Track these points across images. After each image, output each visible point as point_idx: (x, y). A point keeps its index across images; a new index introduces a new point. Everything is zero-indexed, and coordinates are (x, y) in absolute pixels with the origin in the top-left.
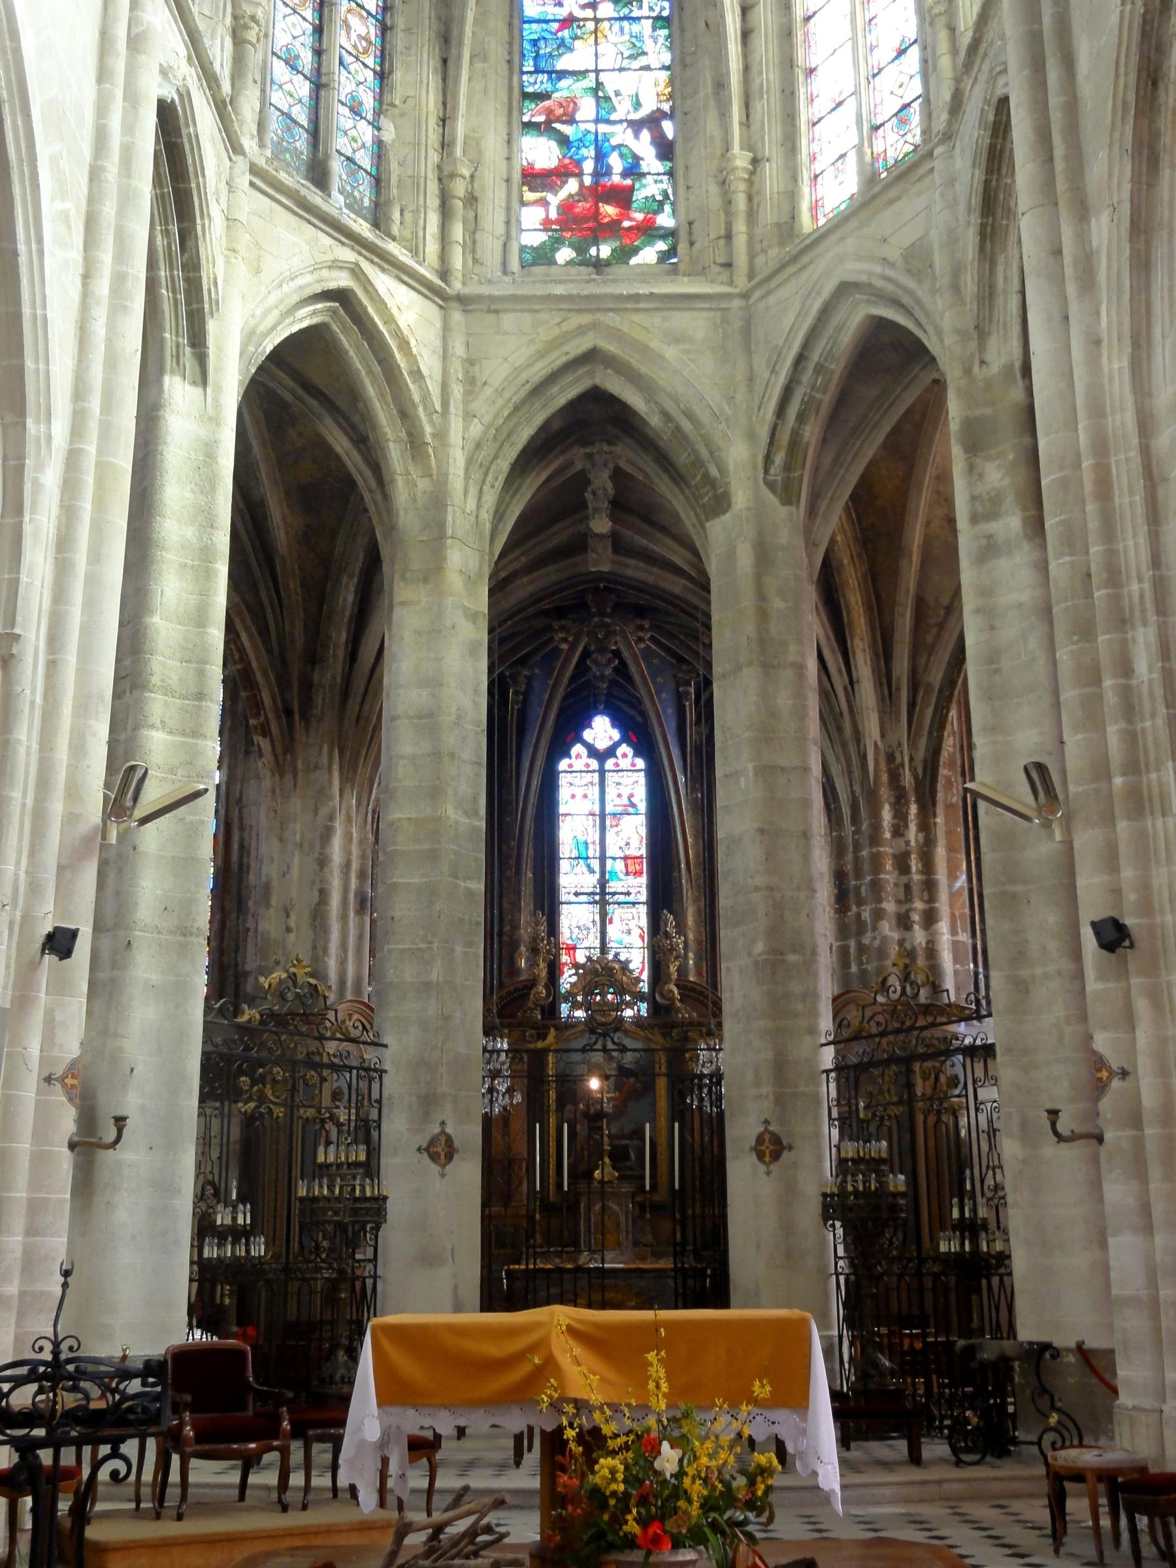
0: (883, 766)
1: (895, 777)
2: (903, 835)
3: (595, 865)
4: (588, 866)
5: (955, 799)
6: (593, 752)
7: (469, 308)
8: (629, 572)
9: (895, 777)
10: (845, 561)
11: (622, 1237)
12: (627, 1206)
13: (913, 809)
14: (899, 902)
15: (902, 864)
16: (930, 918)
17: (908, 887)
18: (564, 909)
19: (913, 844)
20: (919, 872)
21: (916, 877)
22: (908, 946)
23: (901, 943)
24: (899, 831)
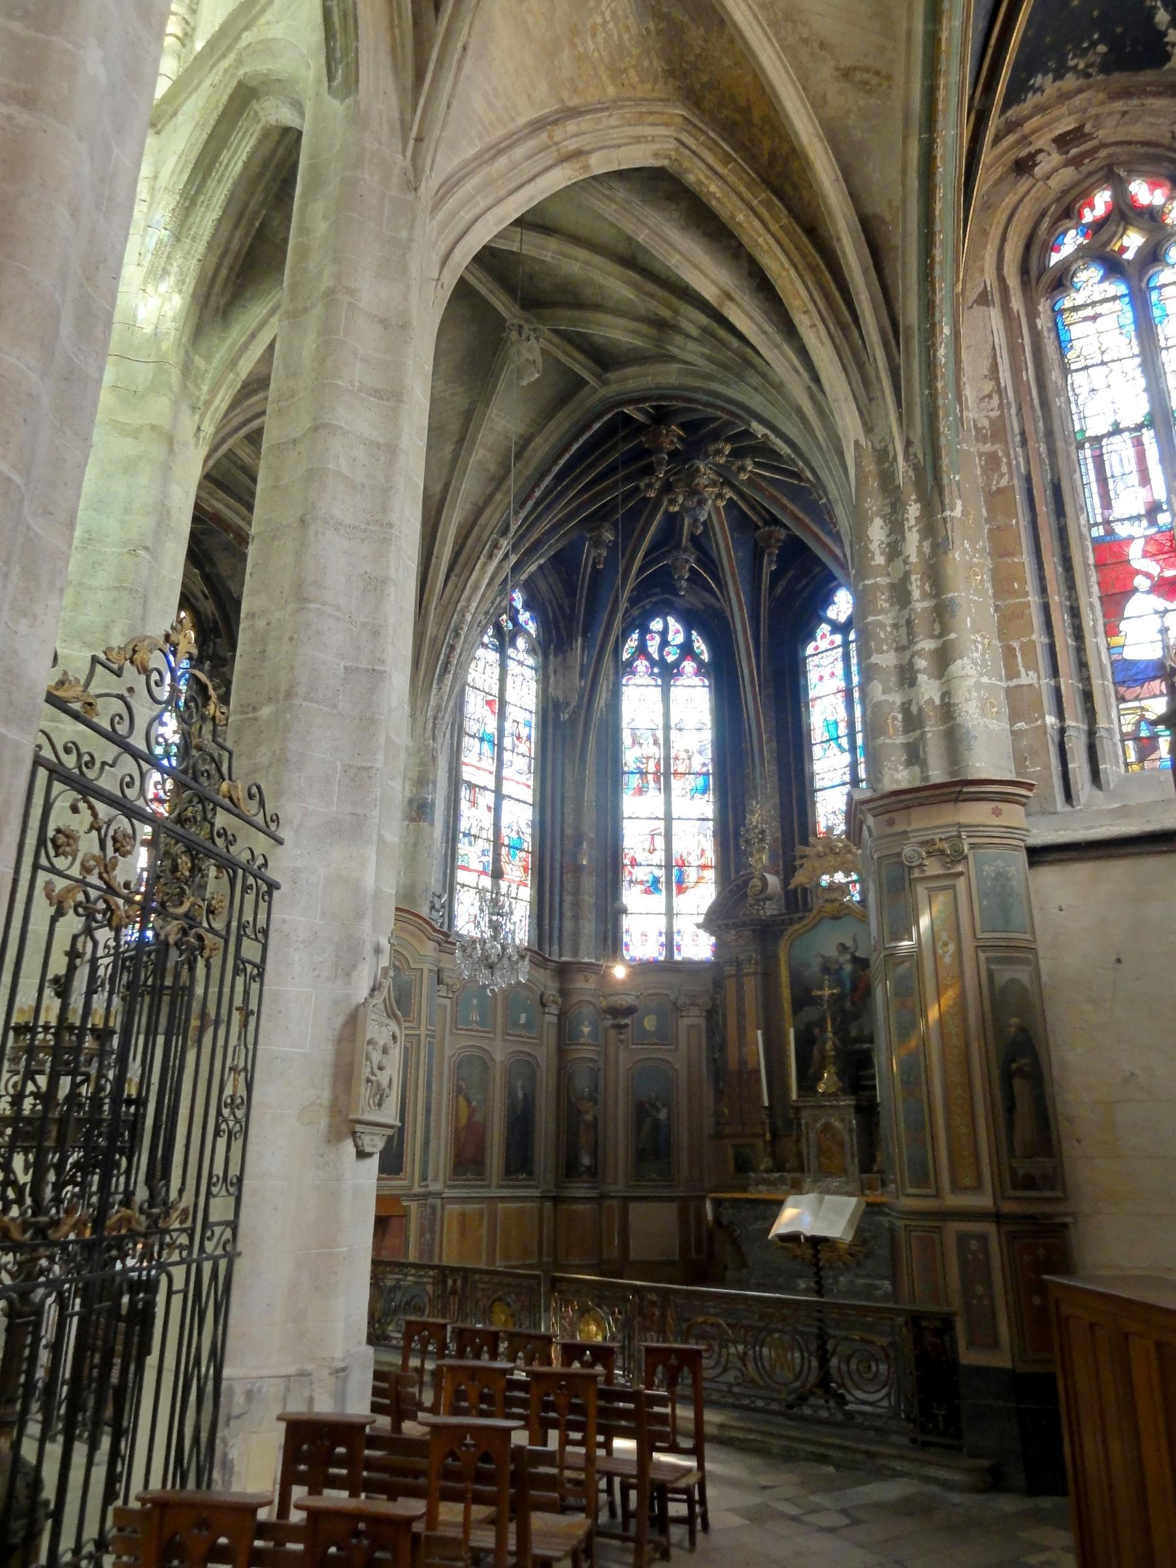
0: (870, 467)
1: (887, 478)
2: (899, 554)
3: (844, 742)
4: (840, 746)
5: (1004, 482)
6: (836, 628)
7: (159, 126)
8: (631, 384)
9: (887, 478)
10: (740, 217)
11: (848, 1160)
12: (850, 1121)
13: (913, 511)
14: (900, 649)
15: (900, 593)
16: (943, 659)
17: (909, 623)
18: (819, 796)
19: (914, 559)
20: (925, 596)
21: (920, 604)
22: (914, 709)
23: (906, 709)
24: (894, 551)
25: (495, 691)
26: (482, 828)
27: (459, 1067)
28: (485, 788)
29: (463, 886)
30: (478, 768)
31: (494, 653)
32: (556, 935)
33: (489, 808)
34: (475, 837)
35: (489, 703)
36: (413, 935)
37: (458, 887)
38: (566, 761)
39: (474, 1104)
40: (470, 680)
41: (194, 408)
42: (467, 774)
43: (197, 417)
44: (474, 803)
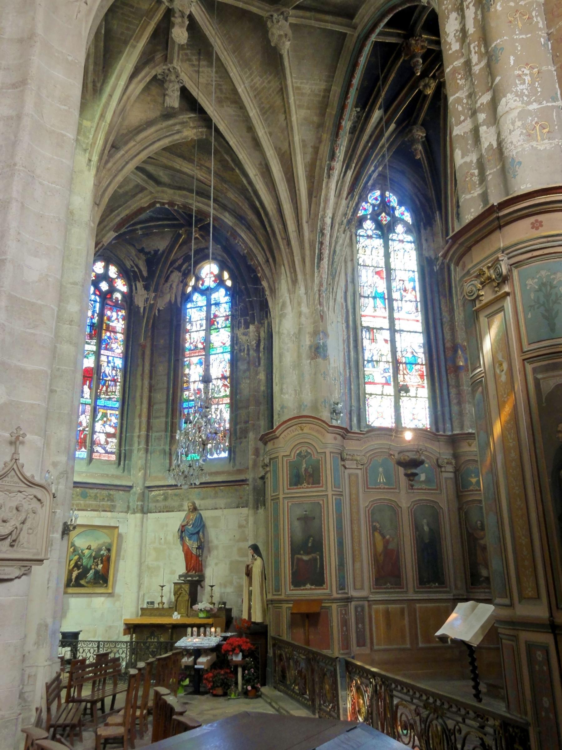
25: (382, 264)
26: (381, 355)
27: (373, 514)
28: (381, 329)
29: (371, 395)
30: (374, 317)
31: (378, 240)
32: (447, 416)
33: (386, 341)
34: (377, 361)
35: (378, 273)
36: (317, 431)
37: (367, 396)
38: (441, 297)
39: (388, 537)
40: (361, 262)
41: (85, 150)
42: (366, 322)
43: (87, 155)
44: (373, 340)
